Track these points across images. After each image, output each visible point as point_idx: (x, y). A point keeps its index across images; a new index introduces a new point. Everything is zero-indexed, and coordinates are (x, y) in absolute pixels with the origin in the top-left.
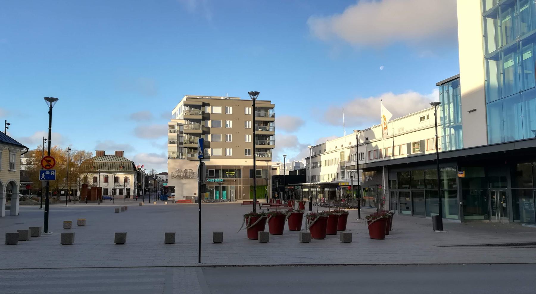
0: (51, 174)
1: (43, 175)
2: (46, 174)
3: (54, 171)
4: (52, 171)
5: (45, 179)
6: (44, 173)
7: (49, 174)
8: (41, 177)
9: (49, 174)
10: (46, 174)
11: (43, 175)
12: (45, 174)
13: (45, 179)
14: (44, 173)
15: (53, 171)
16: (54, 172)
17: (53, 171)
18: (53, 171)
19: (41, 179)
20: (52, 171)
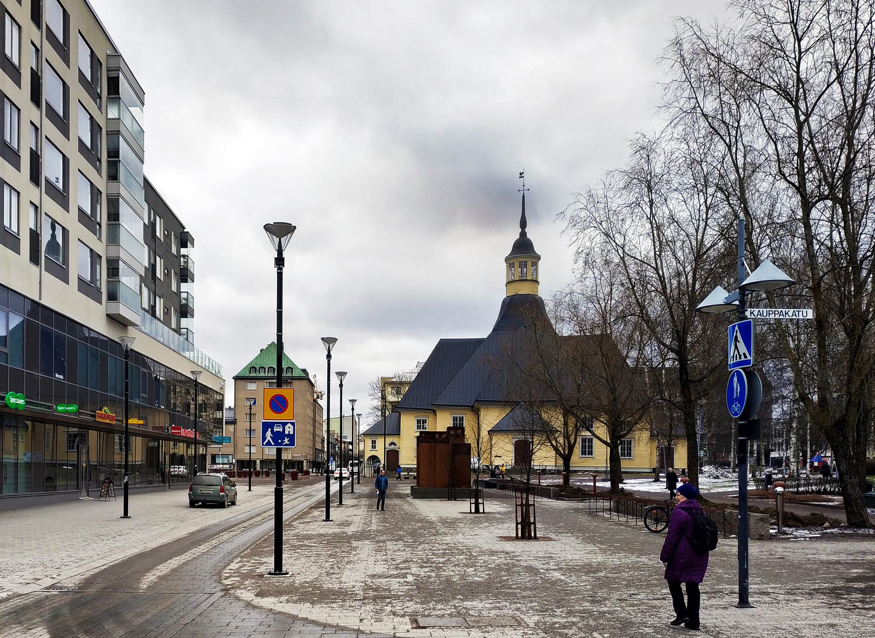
0: (287, 433)
1: (269, 434)
2: (275, 430)
3: (293, 424)
4: (287, 423)
5: (273, 444)
6: (270, 429)
7: (281, 430)
8: (264, 438)
9: (281, 430)
10: (275, 430)
11: (269, 434)
12: (272, 431)
13: (273, 444)
14: (270, 429)
15: (289, 425)
16: (292, 427)
17: (289, 425)
18: (291, 423)
19: (264, 444)
20: (287, 423)
